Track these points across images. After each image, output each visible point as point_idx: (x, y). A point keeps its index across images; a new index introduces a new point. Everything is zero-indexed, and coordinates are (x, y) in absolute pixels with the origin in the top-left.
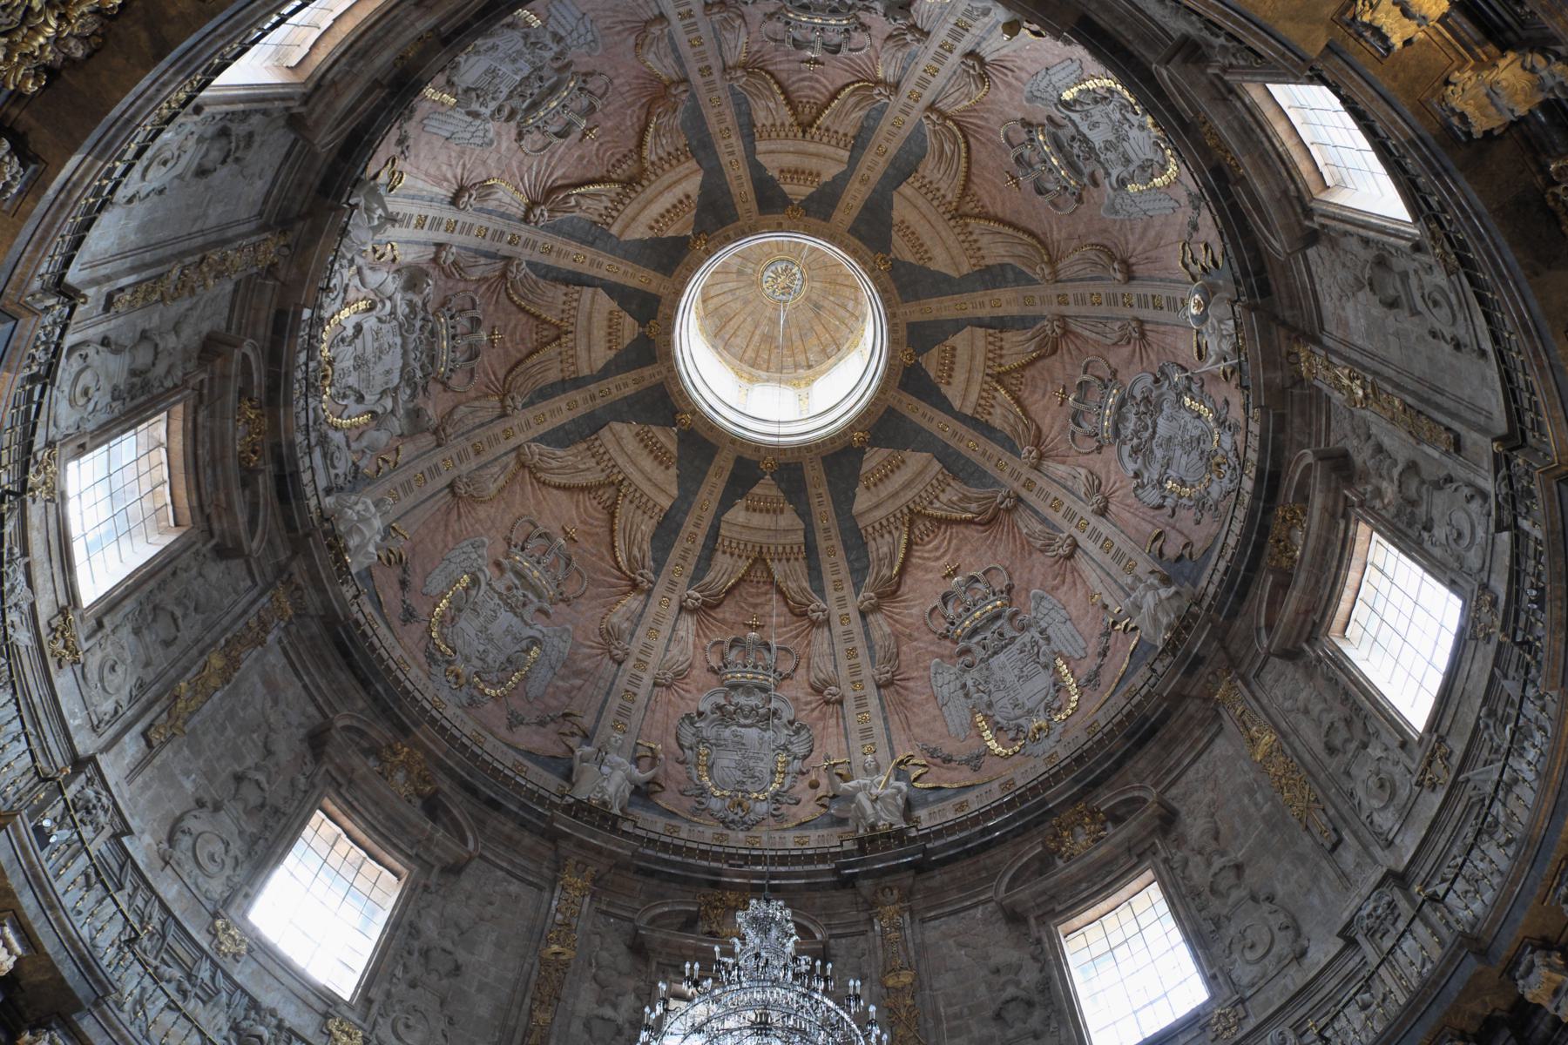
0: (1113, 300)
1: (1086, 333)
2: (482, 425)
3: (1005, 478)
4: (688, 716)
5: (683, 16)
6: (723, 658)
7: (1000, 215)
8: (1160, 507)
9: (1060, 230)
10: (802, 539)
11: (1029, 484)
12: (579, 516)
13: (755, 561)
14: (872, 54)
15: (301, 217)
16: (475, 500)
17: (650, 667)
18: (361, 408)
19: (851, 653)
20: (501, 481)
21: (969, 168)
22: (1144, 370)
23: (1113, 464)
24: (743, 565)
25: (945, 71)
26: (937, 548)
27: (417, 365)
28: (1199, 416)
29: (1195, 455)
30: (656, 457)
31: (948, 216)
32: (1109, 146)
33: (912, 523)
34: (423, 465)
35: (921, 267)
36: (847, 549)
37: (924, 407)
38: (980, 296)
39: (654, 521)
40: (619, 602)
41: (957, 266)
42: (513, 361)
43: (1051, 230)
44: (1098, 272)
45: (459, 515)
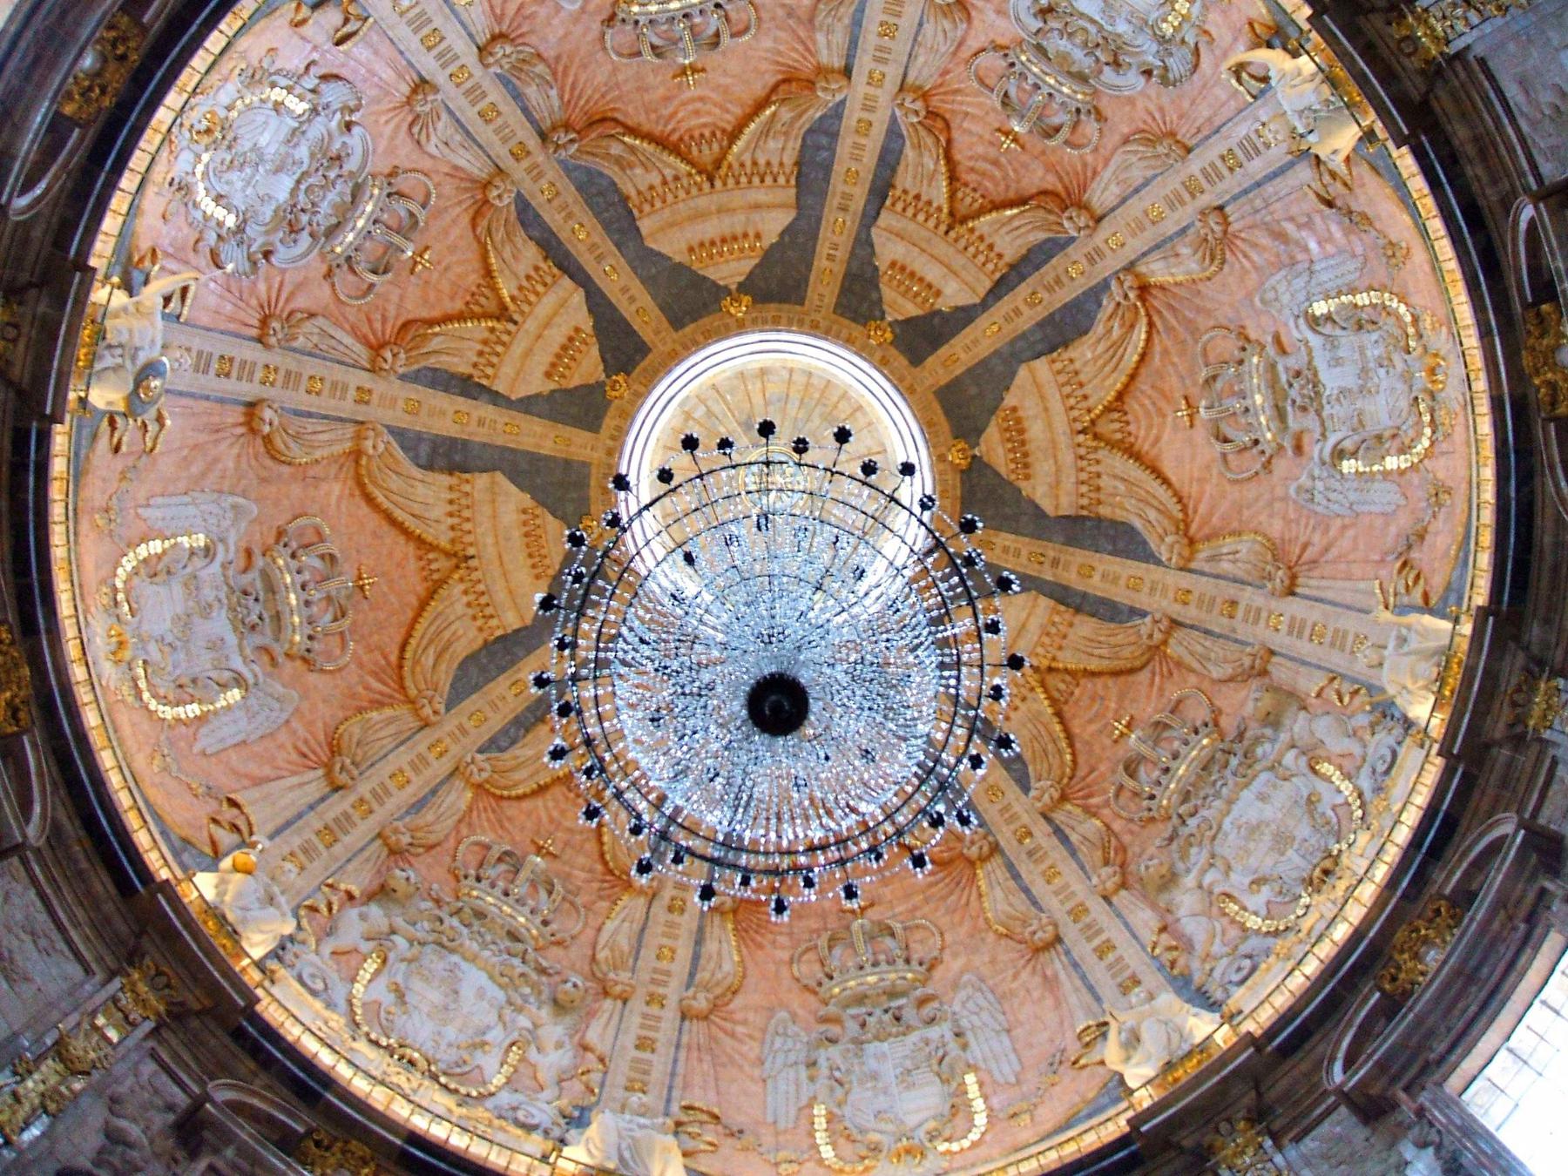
0: (291, 378)
1: (348, 340)
2: (1207, 632)
3: (552, 172)
4: (1165, 81)
5: (660, 1001)
6: (1075, 126)
7: (402, 539)
8: (325, 78)
9: (328, 494)
10: (884, 214)
11: (521, 152)
12: (1162, 426)
13: (964, 221)
14: (464, 831)
15: (1181, 1150)
16: (1276, 551)
17: (1183, 176)
18: (1321, 786)
19: (888, 31)
20: (1228, 545)
21: (415, 620)
22: (283, 271)
23: (380, 150)
24: (984, 223)
25: (385, 769)
26: (697, 113)
27: (1227, 773)
28: (218, 199)
29: (245, 145)
30: (1021, 432)
31: (472, 563)
32: (206, 611)
33: (718, 163)
34: (1304, 648)
35: (543, 504)
36: (827, 168)
37: (626, 310)
38: (480, 435)
39: (1072, 352)
40: (1176, 284)
41: (492, 490)
42: (1122, 679)
43: (340, 499)
44: (295, 424)
45: (1305, 547)
